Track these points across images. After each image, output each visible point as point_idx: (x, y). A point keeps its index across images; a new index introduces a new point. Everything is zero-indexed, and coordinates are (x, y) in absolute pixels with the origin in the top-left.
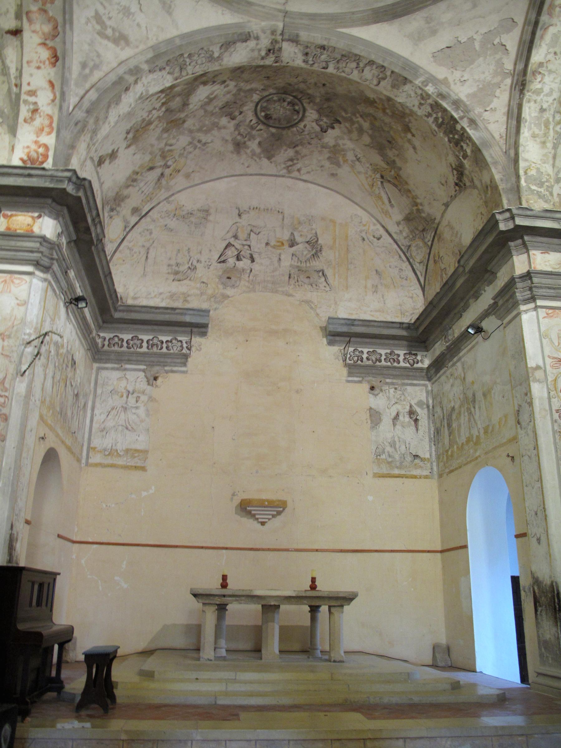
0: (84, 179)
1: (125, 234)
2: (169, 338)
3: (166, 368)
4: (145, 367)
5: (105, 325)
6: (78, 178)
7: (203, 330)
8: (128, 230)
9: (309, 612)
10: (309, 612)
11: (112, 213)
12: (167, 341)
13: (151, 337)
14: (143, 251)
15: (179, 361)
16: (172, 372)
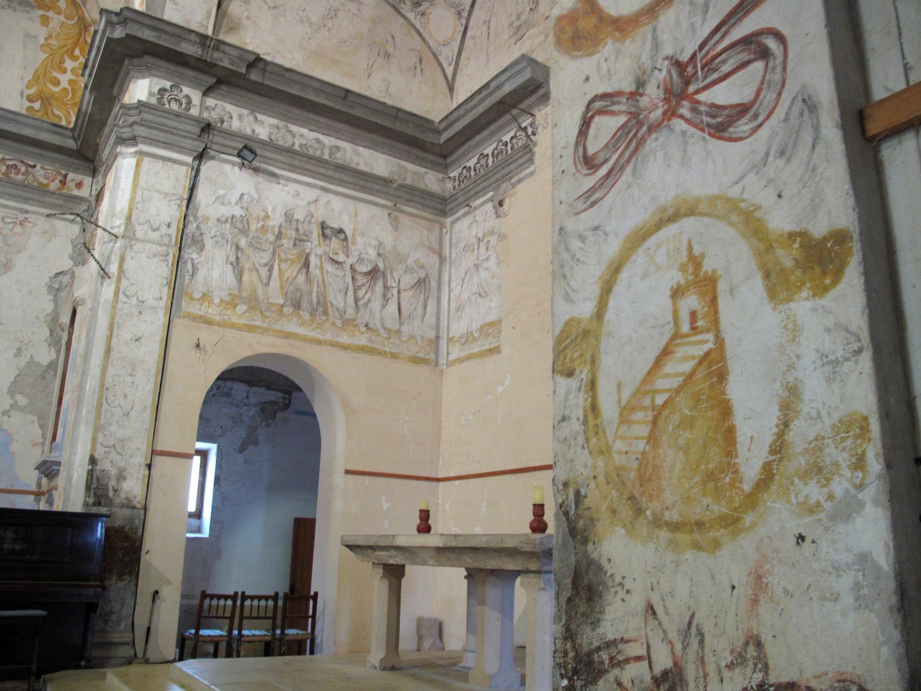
0: (122, 10)
1: (464, 22)
2: (512, 134)
3: (513, 181)
4: (492, 193)
5: (449, 160)
6: (117, 14)
7: (541, 92)
8: (465, 14)
9: (466, 577)
10: (466, 577)
11: (420, 9)
12: (512, 138)
13: (494, 146)
14: (484, 29)
15: (523, 160)
16: (520, 181)
